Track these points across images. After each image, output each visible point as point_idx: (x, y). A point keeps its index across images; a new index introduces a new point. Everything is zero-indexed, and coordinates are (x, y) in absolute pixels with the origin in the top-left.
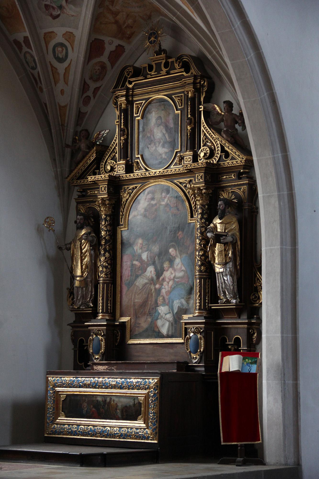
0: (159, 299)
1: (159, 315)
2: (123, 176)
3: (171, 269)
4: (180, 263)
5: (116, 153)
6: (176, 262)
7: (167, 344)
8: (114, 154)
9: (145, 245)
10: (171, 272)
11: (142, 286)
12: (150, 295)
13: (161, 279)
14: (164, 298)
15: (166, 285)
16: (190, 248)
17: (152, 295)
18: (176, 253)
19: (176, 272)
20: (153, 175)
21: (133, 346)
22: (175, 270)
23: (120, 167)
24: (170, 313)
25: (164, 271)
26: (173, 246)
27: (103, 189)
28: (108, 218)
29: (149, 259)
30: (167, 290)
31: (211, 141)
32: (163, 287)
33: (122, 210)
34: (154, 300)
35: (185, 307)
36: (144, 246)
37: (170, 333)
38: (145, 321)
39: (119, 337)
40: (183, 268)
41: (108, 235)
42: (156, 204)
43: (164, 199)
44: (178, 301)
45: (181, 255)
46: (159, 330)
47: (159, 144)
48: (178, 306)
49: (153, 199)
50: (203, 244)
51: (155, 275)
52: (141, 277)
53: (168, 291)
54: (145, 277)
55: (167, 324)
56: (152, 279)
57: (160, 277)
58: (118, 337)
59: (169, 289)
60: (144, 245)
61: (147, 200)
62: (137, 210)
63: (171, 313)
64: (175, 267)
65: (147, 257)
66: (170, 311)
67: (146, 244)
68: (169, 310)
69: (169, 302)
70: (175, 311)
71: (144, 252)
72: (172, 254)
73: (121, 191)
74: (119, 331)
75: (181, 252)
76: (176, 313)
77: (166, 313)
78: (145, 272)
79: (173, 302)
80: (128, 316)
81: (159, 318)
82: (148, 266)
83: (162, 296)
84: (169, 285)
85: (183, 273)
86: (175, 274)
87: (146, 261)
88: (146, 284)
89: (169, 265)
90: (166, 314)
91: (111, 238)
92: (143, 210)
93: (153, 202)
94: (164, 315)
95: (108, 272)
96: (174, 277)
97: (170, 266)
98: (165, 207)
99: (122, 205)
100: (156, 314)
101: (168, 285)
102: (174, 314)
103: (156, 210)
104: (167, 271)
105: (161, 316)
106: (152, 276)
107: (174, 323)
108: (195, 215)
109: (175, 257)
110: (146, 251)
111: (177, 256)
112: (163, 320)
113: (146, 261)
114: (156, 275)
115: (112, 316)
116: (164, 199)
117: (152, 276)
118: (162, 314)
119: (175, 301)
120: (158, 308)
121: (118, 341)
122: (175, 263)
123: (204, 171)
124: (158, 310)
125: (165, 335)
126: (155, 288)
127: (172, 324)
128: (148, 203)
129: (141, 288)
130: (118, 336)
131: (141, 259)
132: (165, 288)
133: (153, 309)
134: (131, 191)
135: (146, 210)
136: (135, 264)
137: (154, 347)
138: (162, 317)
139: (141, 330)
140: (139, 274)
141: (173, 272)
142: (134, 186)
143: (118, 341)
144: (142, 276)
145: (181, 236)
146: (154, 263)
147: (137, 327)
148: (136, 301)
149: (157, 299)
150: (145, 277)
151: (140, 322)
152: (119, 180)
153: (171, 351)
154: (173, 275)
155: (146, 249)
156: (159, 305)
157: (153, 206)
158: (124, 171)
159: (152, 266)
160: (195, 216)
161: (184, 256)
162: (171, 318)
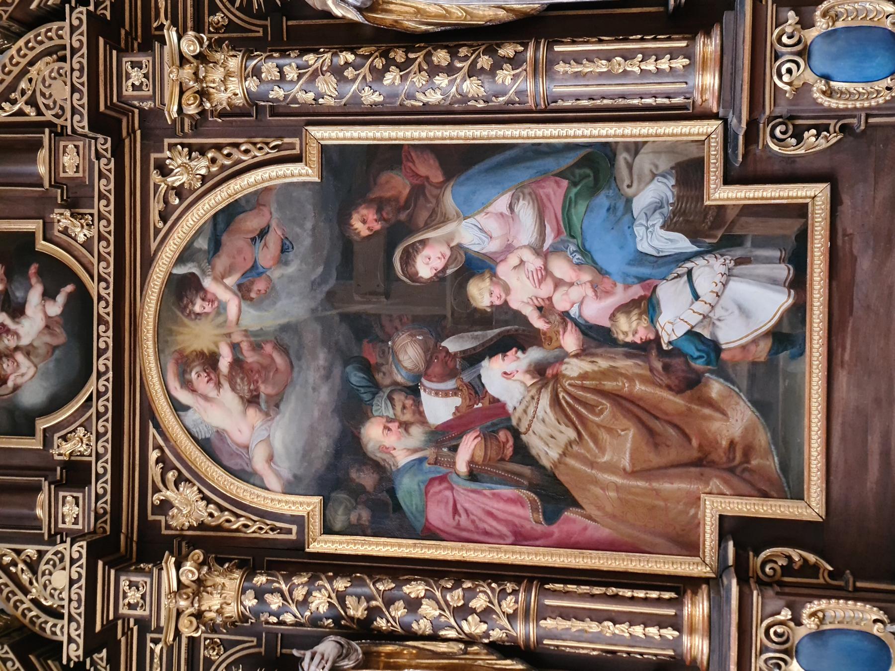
0: (625, 334)
1: (699, 336)
2: (98, 497)
3: (502, 270)
4: (481, 219)
5: (18, 552)
6: (476, 241)
7: (834, 284)
8: (21, 566)
9: (393, 409)
10: (515, 267)
11: (563, 428)
12: (609, 385)
13: (538, 323)
14: (626, 308)
15: (567, 293)
16: (423, 170)
17: (605, 374)
18: (437, 240)
19: (516, 244)
20: (110, 333)
21: (835, 494)
22: (509, 249)
23: (63, 516)
24: (689, 273)
25: (506, 302)
26: (408, 258)
27: (133, 596)
28: (260, 580)
29: (451, 384)
30: (590, 292)
31: (24, 72)
32: (574, 312)
33: (243, 521)
34: (629, 362)
35: (669, 194)
36: (399, 408)
37: (783, 271)
38: (724, 413)
39: (796, 554)
40: (502, 203)
41: (330, 580)
42: (235, 347)
43: (220, 302)
44: (639, 231)
45: (445, 220)
46: (766, 334)
47: (8, 331)
48: (662, 227)
49: (210, 361)
50: (406, 53)
51: (520, 353)
52: (528, 430)
53: (594, 286)
54: (525, 411)
55: (739, 288)
56: (539, 370)
57: (531, 325)
58: (797, 559)
59: (586, 277)
60: (391, 414)
61: (212, 392)
62: (247, 447)
63: (689, 265)
64: (491, 247)
65: (446, 394)
66: (681, 271)
67: (390, 398)
68: (679, 276)
69: (641, 280)
70: (682, 243)
71: (421, 414)
72: (440, 264)
73: (164, 532)
74: (763, 555)
75: (437, 219)
76: (693, 236)
77: (690, 297)
78: (503, 406)
79: (642, 258)
80: (692, 512)
81: (713, 334)
82: (476, 390)
83: (613, 317)
84: (567, 279)
85: (521, 202)
86: (525, 246)
87: (457, 401)
88: (556, 402)
89: (483, 280)
90: (696, 297)
91: (344, 576)
92: (252, 412)
93: (224, 364)
94: (699, 306)
95: (493, 590)
96: (537, 250)
97: (487, 271)
98: (251, 299)
99: (219, 528)
100: (690, 349)
101: (571, 284)
102: (695, 249)
103: (257, 347)
104: (507, 290)
105: (701, 321)
106: (528, 372)
107: (739, 252)
108: (292, 146)
109: (452, 249)
110: (418, 403)
111: (447, 240)
112: (718, 312)
113: (457, 401)
114: (524, 350)
115: (695, 593)
116: (216, 304)
117: (528, 372)
118: (694, 319)
119: (640, 248)
120: (665, 339)
121: (812, 558)
122: (476, 248)
123: (114, 52)
124: (674, 338)
125: (791, 301)
126: (576, 356)
127: (739, 262)
128: (226, 385)
129: (572, 434)
130: (789, 557)
131: (446, 427)
132: (582, 303)
133: (666, 368)
134: (171, 476)
135: (252, 400)
136: (471, 462)
137: (842, 362)
138: (705, 317)
139: (763, 438)
140: (511, 443)
141: (513, 260)
142: (154, 455)
143: (812, 558)
144: (522, 429)
145: (371, 214)
146: (473, 358)
147: (748, 462)
148: (626, 462)
149: (627, 345)
150: (525, 411)
151: (724, 443)
152: (108, 516)
153: (865, 264)
154: (528, 256)
155: (409, 402)
156: (652, 336)
157: (237, 363)
158: (80, 495)
159: (483, 372)
160: (298, 147)
161: (449, 201)
162: (712, 267)
